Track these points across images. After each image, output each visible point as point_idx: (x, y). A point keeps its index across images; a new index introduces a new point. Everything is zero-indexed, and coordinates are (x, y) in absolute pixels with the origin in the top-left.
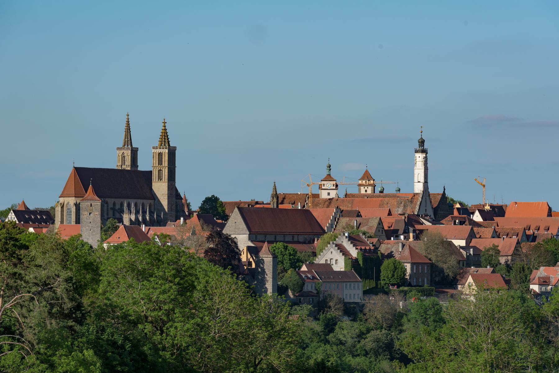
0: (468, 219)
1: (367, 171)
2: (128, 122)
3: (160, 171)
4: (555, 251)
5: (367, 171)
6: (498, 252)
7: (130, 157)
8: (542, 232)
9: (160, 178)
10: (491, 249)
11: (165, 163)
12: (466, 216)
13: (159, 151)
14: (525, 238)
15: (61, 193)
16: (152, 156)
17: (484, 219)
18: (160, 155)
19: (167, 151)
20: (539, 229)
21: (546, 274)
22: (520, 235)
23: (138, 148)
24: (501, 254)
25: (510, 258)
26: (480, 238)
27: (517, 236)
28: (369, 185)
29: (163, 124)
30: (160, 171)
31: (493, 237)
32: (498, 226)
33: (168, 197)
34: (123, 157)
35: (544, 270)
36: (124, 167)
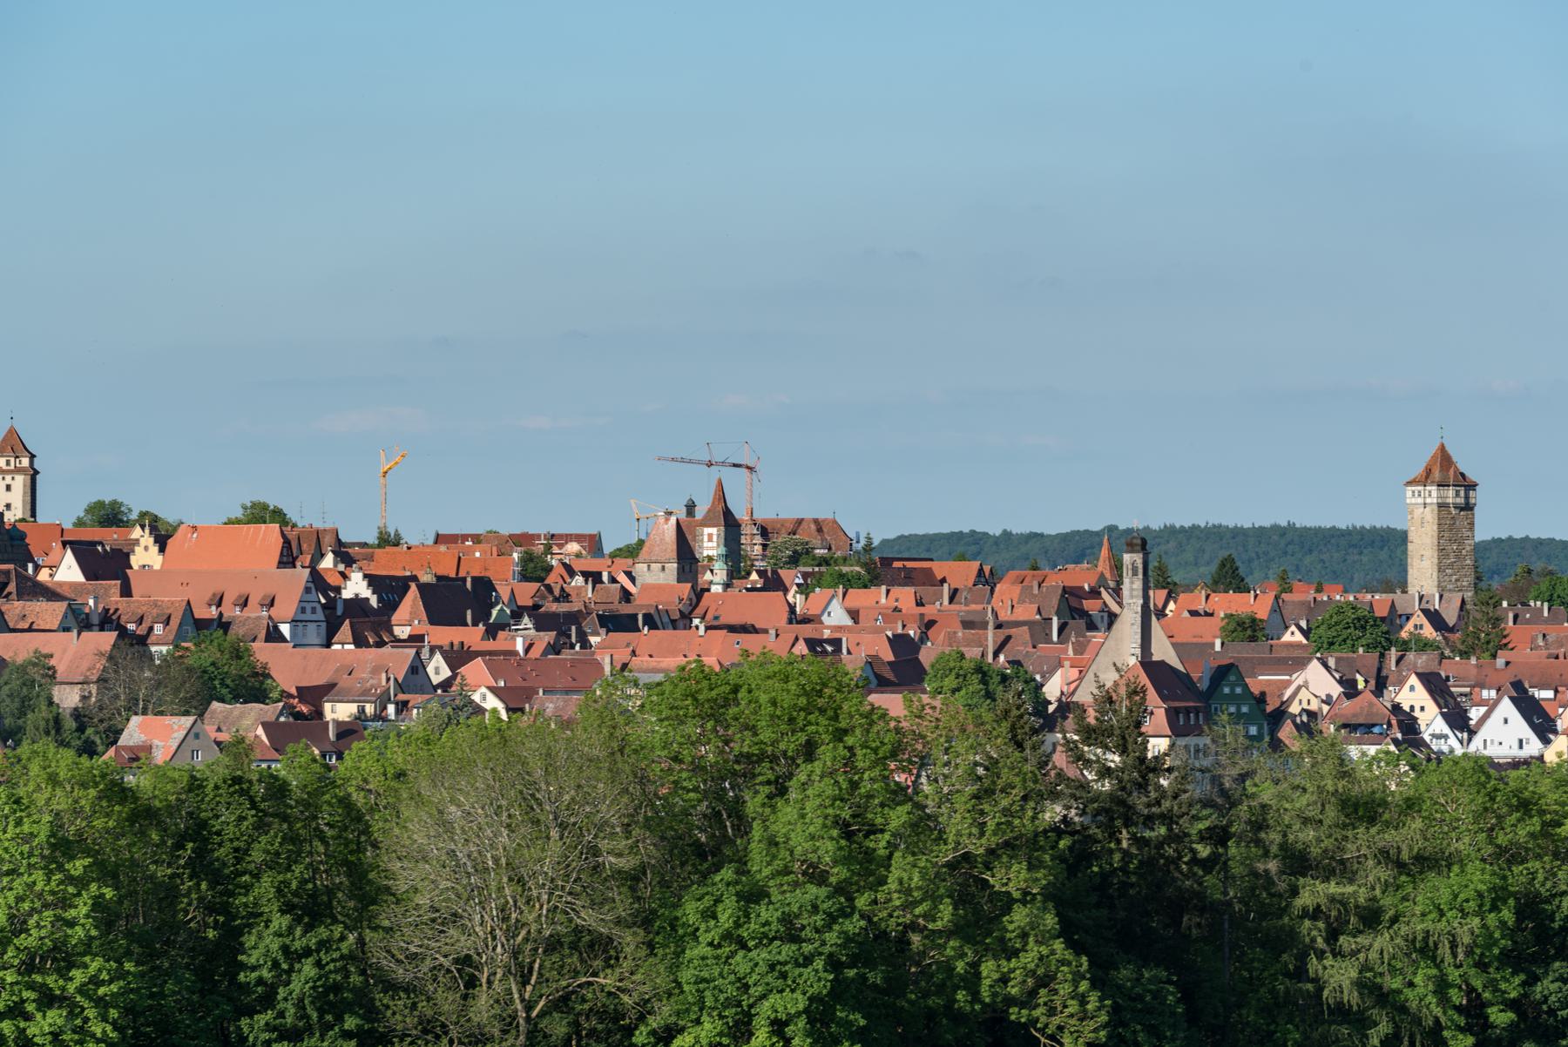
0: (18, 575)
1: (12, 432)
4: (211, 669)
5: (12, 432)
6: (51, 674)
8: (256, 613)
10: (35, 665)
12: (11, 566)
14: (190, 628)
17: (90, 574)
20: (245, 604)
21: (143, 738)
22: (175, 622)
24: (59, 677)
25: (94, 688)
26: (30, 630)
27: (167, 622)
28: (18, 470)
31: (67, 629)
32: (126, 591)
35: (140, 726)
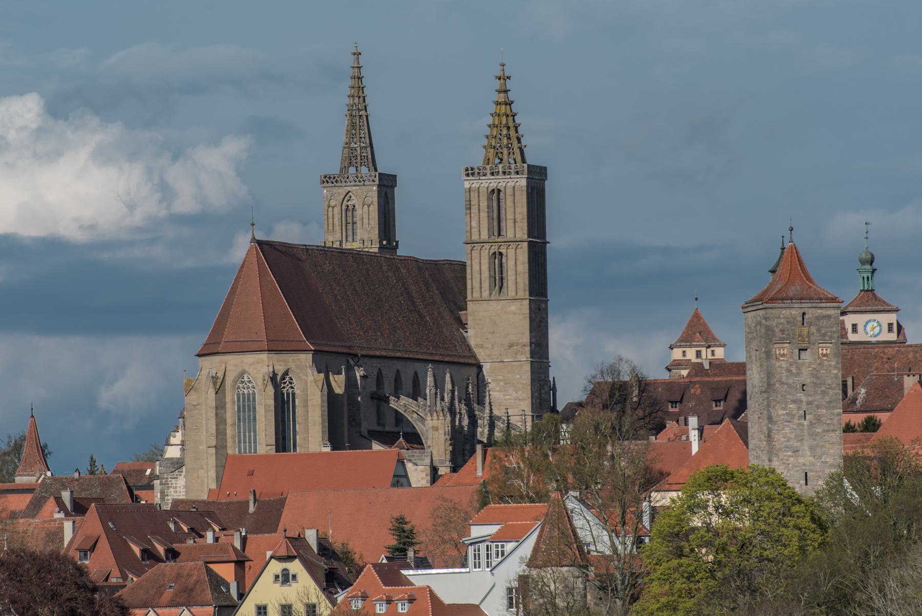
2: (360, 78)
3: (498, 256)
7: (374, 209)
9: (498, 281)
11: (516, 225)
13: (493, 183)
15: (204, 338)
16: (463, 204)
18: (496, 193)
19: (523, 182)
23: (393, 178)
29: (497, 84)
30: (498, 256)
33: (533, 354)
34: (349, 210)
36: (347, 246)
